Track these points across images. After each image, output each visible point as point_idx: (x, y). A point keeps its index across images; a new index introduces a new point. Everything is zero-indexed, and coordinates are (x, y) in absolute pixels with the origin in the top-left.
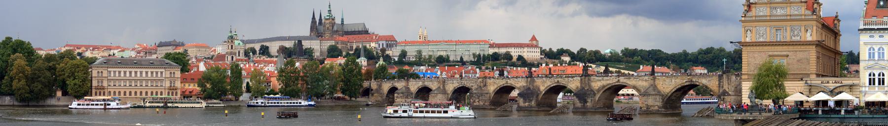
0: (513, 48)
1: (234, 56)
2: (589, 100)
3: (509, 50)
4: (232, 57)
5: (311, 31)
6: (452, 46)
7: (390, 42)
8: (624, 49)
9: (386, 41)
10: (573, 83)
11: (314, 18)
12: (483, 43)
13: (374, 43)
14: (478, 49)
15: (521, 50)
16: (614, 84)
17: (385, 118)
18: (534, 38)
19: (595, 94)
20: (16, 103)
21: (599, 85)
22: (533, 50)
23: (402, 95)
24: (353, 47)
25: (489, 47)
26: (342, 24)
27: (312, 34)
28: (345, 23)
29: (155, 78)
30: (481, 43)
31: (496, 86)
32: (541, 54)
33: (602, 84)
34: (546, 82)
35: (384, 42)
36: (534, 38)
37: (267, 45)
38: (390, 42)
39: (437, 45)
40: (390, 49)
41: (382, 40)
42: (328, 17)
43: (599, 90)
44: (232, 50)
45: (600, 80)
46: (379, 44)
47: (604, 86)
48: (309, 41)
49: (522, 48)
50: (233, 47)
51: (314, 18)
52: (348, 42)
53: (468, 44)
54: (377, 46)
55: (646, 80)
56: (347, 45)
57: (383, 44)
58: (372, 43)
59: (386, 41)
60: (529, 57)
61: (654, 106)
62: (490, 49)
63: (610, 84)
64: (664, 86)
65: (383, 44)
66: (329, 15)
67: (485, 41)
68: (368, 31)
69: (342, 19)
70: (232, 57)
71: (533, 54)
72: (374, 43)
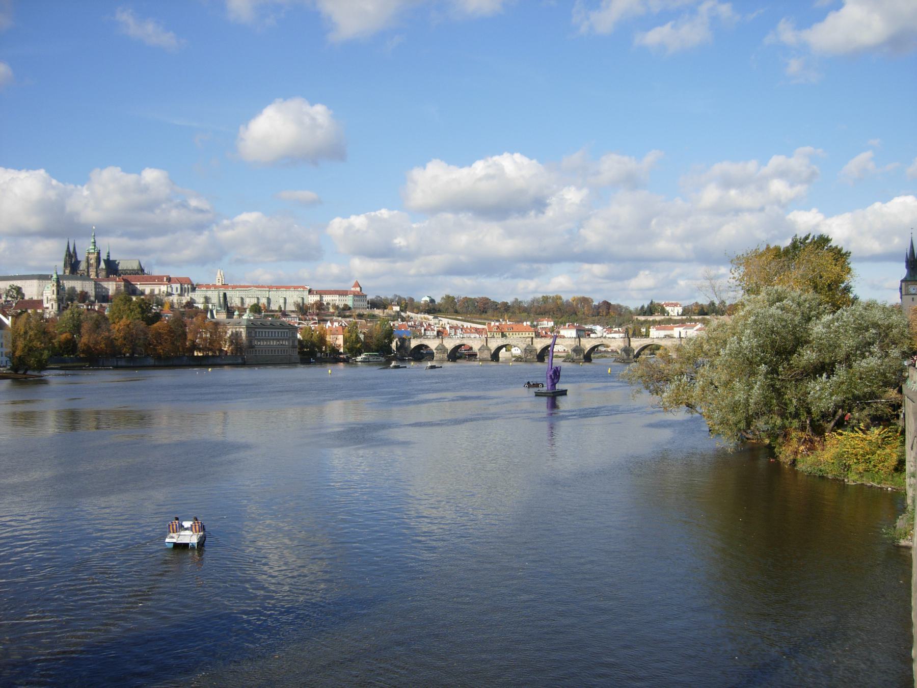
0: (337, 296)
2: (631, 354)
6: (264, 292)
8: (444, 296)
11: (68, 248)
12: (302, 289)
23: (440, 351)
37: (18, 285)
38: (186, 286)
39: (246, 290)
41: (175, 283)
42: (93, 251)
43: (637, 348)
45: (638, 341)
48: (81, 282)
51: (68, 248)
57: (177, 288)
58: (162, 286)
62: (310, 296)
65: (177, 288)
68: (142, 270)
69: (109, 253)
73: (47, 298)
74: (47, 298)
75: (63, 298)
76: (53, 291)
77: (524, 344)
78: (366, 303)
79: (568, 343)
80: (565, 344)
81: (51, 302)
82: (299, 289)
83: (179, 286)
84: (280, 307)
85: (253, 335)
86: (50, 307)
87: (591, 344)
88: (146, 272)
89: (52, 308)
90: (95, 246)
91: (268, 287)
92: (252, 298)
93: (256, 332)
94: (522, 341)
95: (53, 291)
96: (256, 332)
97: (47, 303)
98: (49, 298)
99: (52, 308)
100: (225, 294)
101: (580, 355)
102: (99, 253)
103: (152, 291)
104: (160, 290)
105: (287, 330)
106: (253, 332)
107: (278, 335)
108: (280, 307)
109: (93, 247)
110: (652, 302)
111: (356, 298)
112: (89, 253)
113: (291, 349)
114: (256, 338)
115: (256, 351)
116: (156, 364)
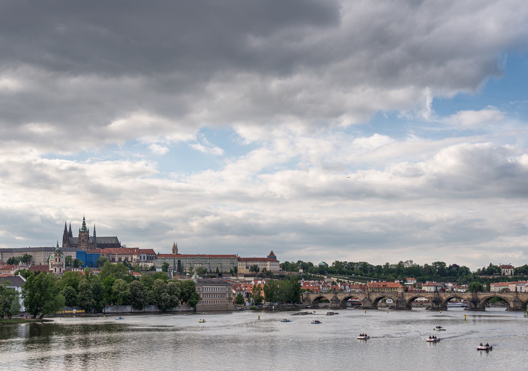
0: (258, 262)
1: (61, 268)
2: (478, 304)
3: (256, 264)
4: (60, 269)
5: (63, 242)
7: (150, 255)
9: (147, 254)
10: (466, 296)
12: (233, 257)
13: (136, 256)
14: (229, 262)
15: (264, 264)
16: (492, 296)
17: (200, 323)
18: (272, 253)
19: (480, 301)
20: (158, 310)
21: (482, 297)
22: (273, 264)
23: (334, 302)
24: (115, 258)
25: (238, 261)
26: (95, 237)
27: (65, 245)
28: (97, 236)
29: (214, 292)
30: (231, 257)
31: (410, 297)
32: (280, 267)
33: (484, 296)
34: (447, 295)
35: (145, 255)
36: (272, 253)
38: (150, 255)
39: (193, 258)
40: (150, 261)
41: (143, 253)
43: (482, 299)
44: (56, 263)
45: (483, 294)
46: (141, 257)
47: (485, 297)
49: (265, 262)
50: (61, 260)
52: (110, 254)
53: (220, 258)
54: (139, 258)
55: (512, 295)
56: (109, 256)
57: (144, 257)
58: (134, 256)
59: (147, 254)
60: (271, 269)
61: (518, 307)
62: (238, 262)
63: (490, 296)
64: (522, 297)
65: (144, 257)
66: (84, 228)
67: (234, 256)
69: (95, 232)
70: (60, 269)
71: (275, 267)
72: (136, 256)
73: (52, 264)
74: (52, 264)
75: (63, 264)
76: (56, 258)
77: (396, 296)
78: (279, 267)
79: (429, 296)
80: (427, 297)
81: (55, 267)
82: (231, 257)
83: (145, 255)
84: (218, 270)
85: (201, 290)
86: (54, 271)
87: (447, 297)
88: (122, 245)
89: (55, 271)
90: (85, 227)
91: (209, 256)
92: (198, 263)
93: (203, 288)
94: (395, 294)
95: (56, 258)
96: (203, 288)
97: (52, 268)
98: (53, 264)
99: (55, 271)
100: (179, 261)
101: (438, 305)
102: (88, 232)
103: (127, 259)
104: (132, 258)
105: (226, 287)
106: (201, 288)
107: (219, 290)
108: (218, 270)
109: (84, 228)
110: (491, 263)
111: (271, 264)
112: (81, 232)
113: (227, 300)
114: (203, 292)
115: (203, 301)
116: (133, 311)
